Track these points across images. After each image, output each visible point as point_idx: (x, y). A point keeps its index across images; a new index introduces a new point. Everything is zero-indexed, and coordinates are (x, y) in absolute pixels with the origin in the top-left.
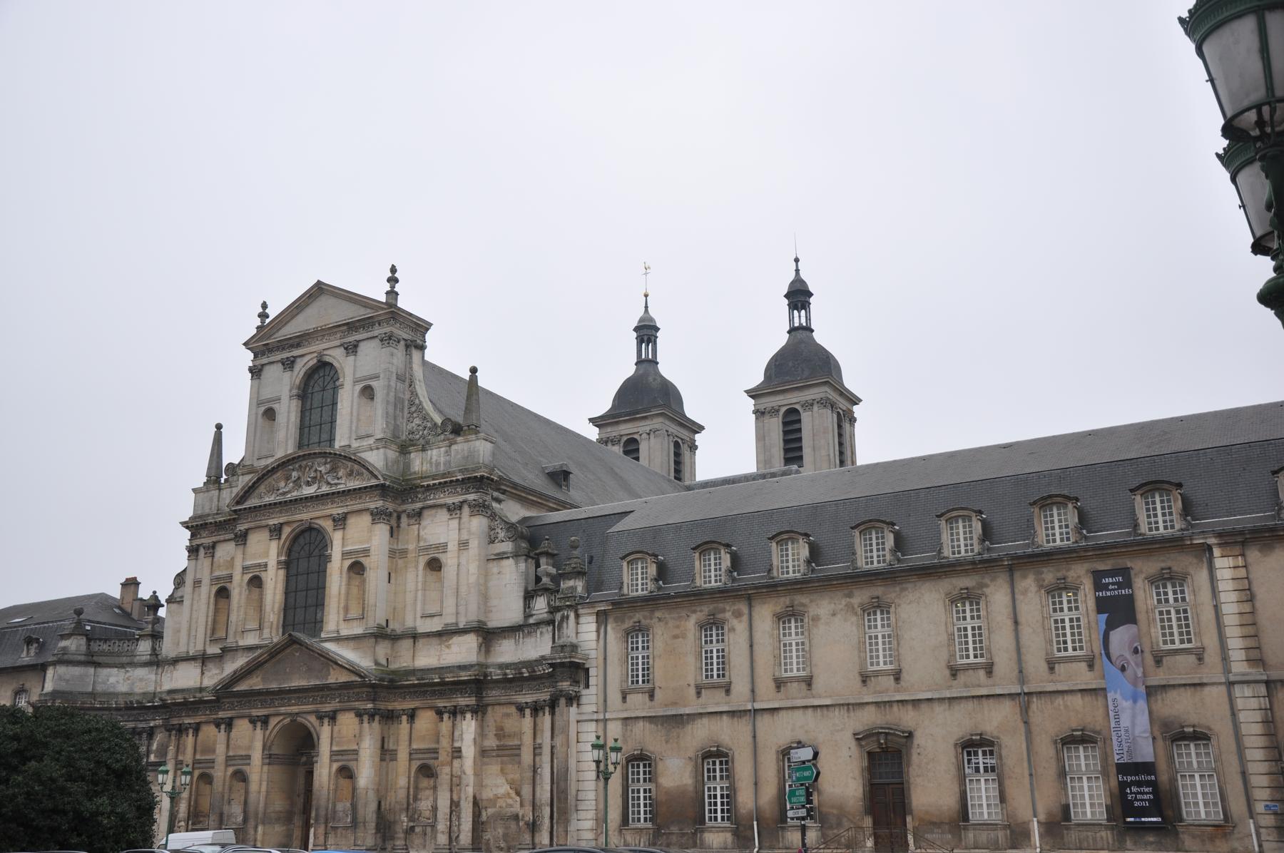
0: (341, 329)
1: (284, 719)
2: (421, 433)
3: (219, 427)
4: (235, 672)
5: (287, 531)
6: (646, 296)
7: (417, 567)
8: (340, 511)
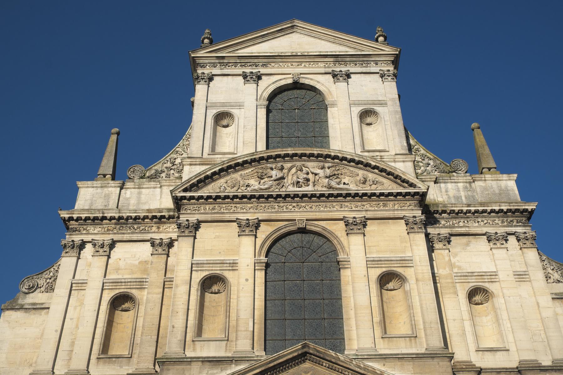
2: (422, 168)
5: (265, 231)
7: (456, 293)
8: (359, 215)
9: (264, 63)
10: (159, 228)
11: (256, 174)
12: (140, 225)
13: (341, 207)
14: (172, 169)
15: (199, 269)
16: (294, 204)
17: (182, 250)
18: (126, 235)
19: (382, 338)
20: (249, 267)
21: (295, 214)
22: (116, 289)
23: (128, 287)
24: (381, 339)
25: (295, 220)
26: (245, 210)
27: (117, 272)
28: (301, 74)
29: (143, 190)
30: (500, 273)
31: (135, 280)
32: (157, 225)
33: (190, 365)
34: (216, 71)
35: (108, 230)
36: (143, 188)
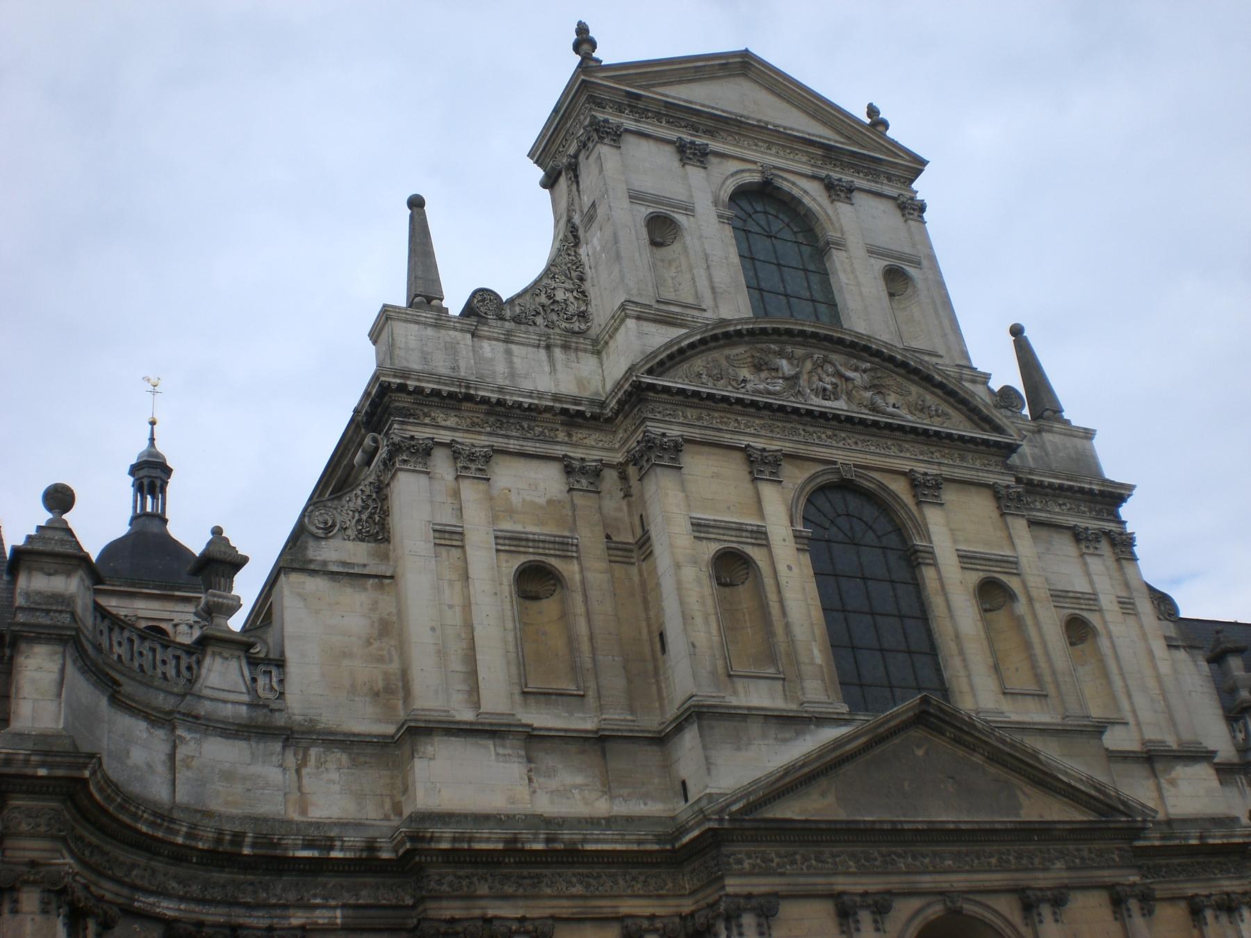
0: (811, 150)
1: (928, 905)
3: (416, 204)
4: (787, 771)
6: (153, 423)
9: (708, 128)
10: (570, 435)
11: (749, 360)
12: (533, 424)
13: (901, 451)
14: (553, 310)
15: (703, 535)
16: (829, 433)
17: (667, 494)
18: (512, 441)
19: (1004, 693)
20: (787, 544)
21: (835, 452)
22: (519, 552)
23: (541, 551)
24: (1001, 696)
25: (835, 463)
26: (752, 429)
27: (511, 517)
28: (775, 168)
29: (514, 347)
30: (1101, 597)
31: (552, 539)
32: (566, 428)
33: (746, 721)
34: (630, 124)
35: (473, 424)
36: (512, 342)
